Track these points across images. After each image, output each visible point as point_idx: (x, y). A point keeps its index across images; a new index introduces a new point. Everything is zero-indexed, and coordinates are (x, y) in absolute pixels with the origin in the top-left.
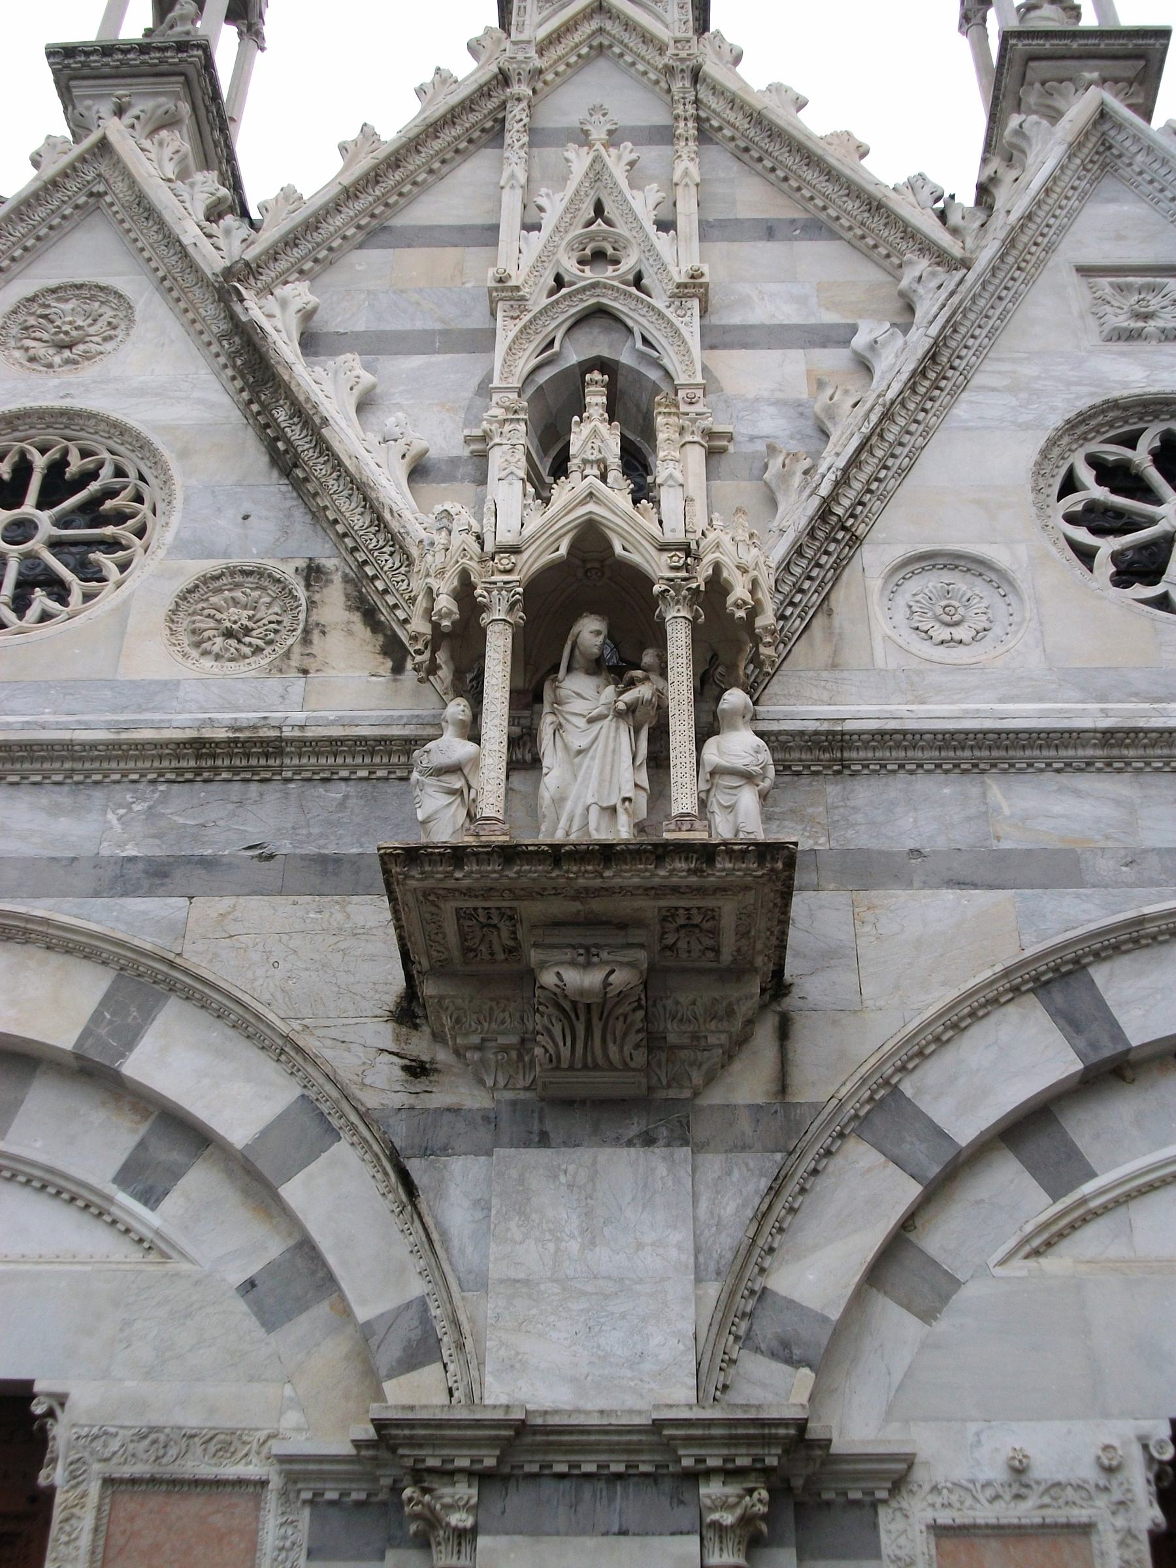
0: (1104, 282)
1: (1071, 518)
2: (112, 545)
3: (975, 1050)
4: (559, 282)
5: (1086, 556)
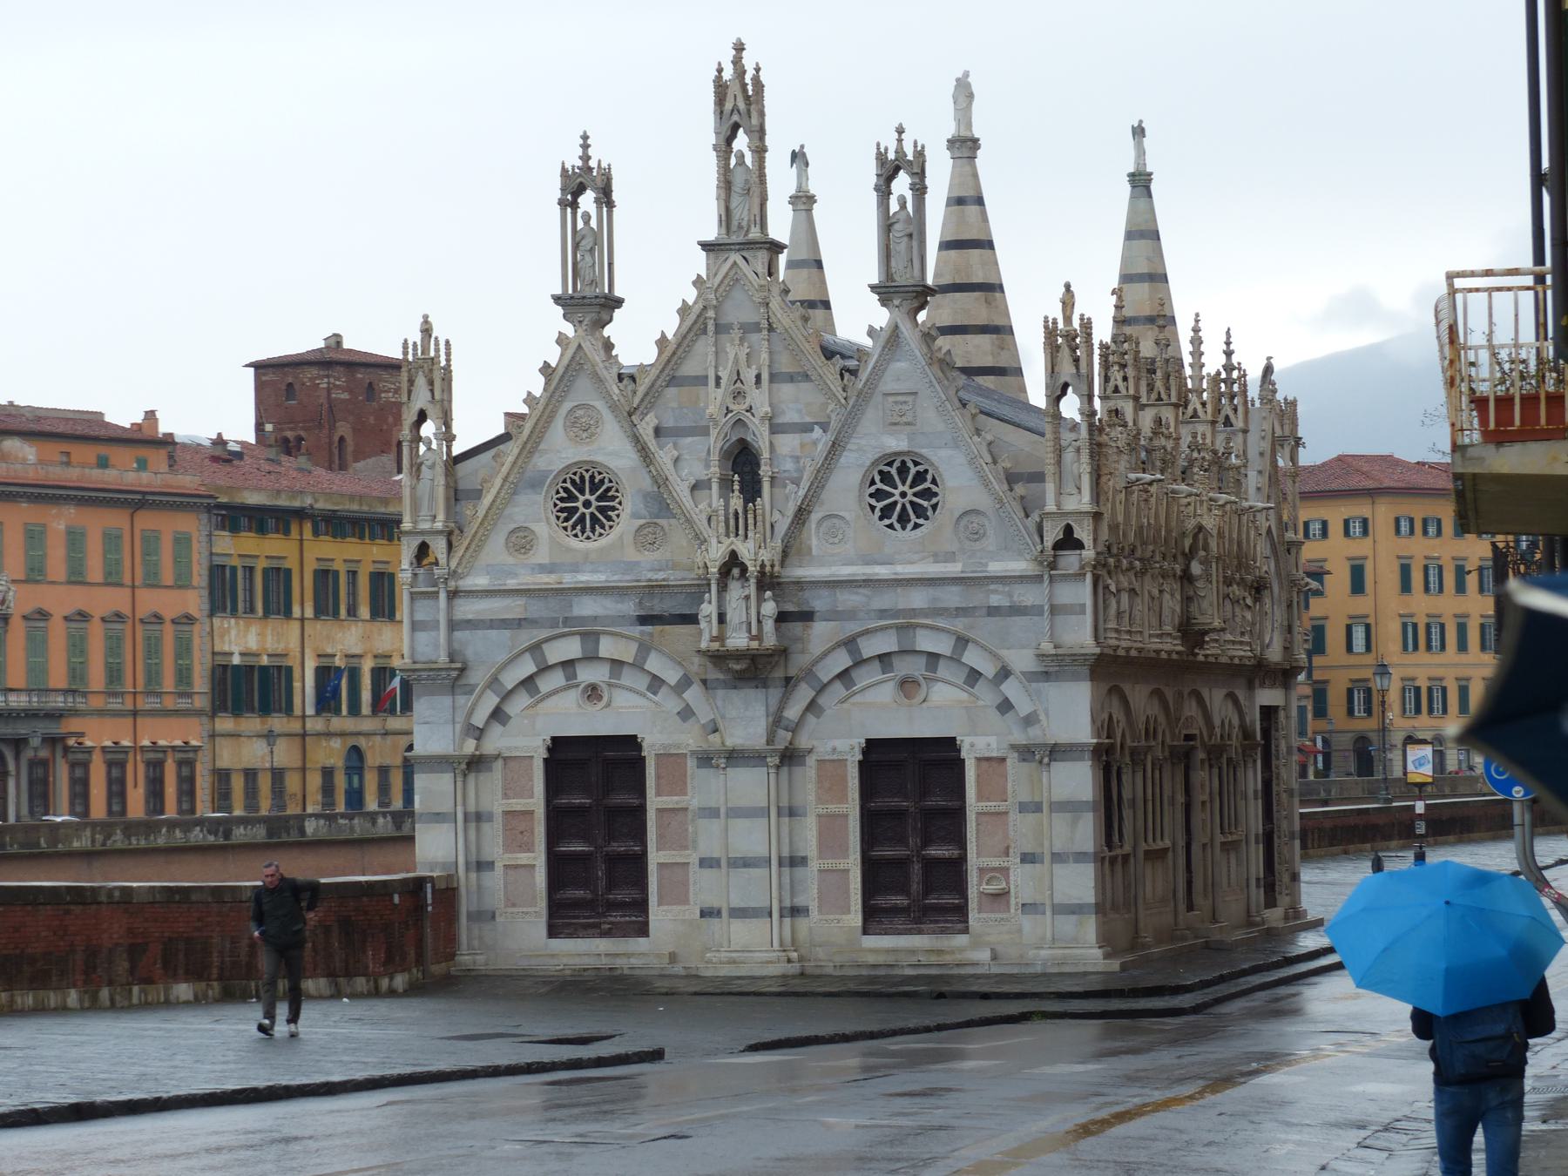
0: (891, 399)
1: (871, 495)
2: (613, 509)
3: (829, 660)
4: (728, 411)
5: (873, 508)
